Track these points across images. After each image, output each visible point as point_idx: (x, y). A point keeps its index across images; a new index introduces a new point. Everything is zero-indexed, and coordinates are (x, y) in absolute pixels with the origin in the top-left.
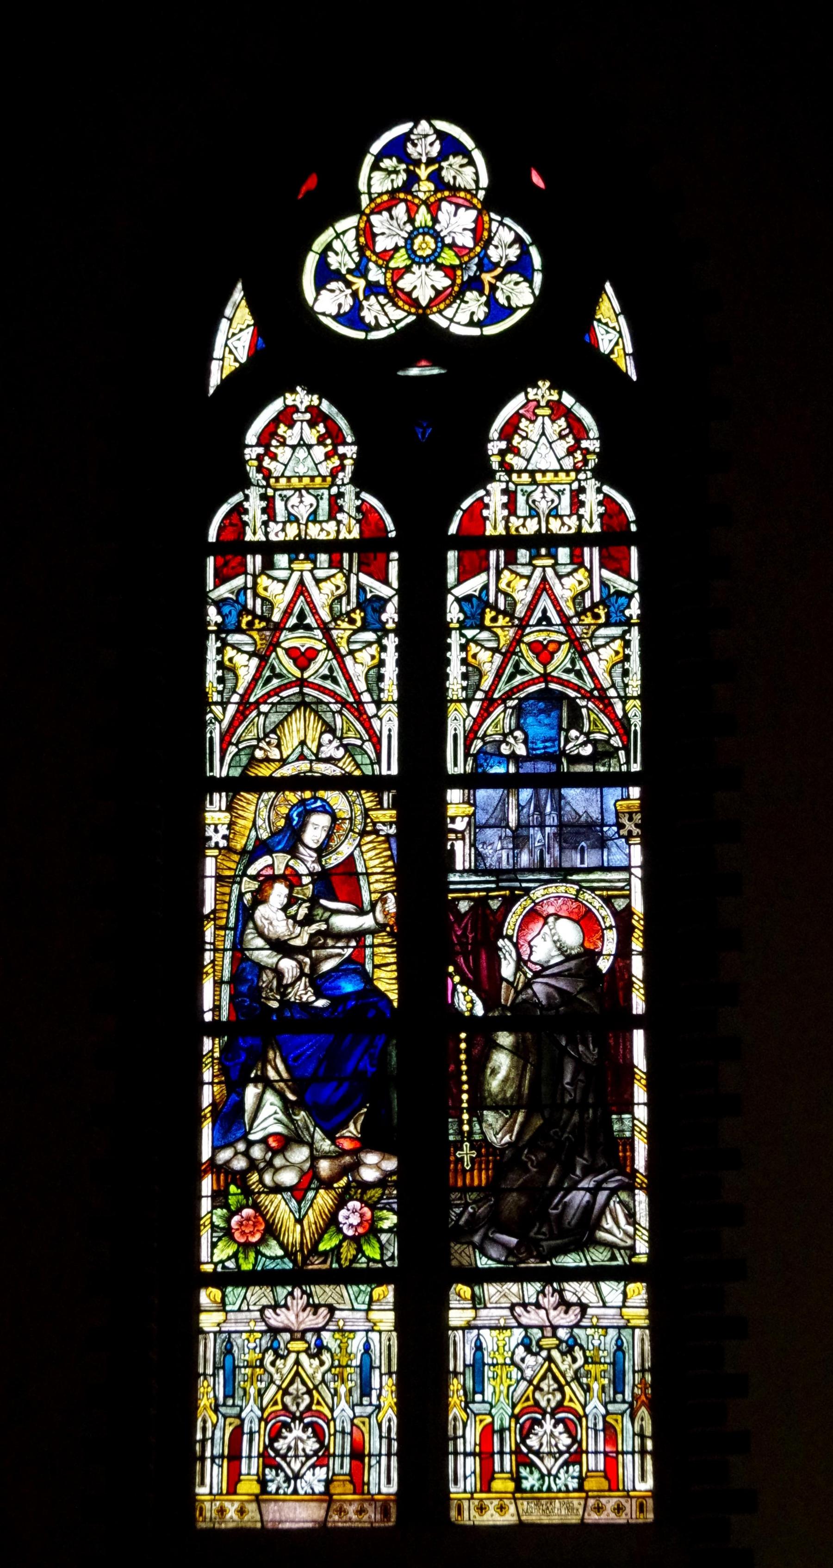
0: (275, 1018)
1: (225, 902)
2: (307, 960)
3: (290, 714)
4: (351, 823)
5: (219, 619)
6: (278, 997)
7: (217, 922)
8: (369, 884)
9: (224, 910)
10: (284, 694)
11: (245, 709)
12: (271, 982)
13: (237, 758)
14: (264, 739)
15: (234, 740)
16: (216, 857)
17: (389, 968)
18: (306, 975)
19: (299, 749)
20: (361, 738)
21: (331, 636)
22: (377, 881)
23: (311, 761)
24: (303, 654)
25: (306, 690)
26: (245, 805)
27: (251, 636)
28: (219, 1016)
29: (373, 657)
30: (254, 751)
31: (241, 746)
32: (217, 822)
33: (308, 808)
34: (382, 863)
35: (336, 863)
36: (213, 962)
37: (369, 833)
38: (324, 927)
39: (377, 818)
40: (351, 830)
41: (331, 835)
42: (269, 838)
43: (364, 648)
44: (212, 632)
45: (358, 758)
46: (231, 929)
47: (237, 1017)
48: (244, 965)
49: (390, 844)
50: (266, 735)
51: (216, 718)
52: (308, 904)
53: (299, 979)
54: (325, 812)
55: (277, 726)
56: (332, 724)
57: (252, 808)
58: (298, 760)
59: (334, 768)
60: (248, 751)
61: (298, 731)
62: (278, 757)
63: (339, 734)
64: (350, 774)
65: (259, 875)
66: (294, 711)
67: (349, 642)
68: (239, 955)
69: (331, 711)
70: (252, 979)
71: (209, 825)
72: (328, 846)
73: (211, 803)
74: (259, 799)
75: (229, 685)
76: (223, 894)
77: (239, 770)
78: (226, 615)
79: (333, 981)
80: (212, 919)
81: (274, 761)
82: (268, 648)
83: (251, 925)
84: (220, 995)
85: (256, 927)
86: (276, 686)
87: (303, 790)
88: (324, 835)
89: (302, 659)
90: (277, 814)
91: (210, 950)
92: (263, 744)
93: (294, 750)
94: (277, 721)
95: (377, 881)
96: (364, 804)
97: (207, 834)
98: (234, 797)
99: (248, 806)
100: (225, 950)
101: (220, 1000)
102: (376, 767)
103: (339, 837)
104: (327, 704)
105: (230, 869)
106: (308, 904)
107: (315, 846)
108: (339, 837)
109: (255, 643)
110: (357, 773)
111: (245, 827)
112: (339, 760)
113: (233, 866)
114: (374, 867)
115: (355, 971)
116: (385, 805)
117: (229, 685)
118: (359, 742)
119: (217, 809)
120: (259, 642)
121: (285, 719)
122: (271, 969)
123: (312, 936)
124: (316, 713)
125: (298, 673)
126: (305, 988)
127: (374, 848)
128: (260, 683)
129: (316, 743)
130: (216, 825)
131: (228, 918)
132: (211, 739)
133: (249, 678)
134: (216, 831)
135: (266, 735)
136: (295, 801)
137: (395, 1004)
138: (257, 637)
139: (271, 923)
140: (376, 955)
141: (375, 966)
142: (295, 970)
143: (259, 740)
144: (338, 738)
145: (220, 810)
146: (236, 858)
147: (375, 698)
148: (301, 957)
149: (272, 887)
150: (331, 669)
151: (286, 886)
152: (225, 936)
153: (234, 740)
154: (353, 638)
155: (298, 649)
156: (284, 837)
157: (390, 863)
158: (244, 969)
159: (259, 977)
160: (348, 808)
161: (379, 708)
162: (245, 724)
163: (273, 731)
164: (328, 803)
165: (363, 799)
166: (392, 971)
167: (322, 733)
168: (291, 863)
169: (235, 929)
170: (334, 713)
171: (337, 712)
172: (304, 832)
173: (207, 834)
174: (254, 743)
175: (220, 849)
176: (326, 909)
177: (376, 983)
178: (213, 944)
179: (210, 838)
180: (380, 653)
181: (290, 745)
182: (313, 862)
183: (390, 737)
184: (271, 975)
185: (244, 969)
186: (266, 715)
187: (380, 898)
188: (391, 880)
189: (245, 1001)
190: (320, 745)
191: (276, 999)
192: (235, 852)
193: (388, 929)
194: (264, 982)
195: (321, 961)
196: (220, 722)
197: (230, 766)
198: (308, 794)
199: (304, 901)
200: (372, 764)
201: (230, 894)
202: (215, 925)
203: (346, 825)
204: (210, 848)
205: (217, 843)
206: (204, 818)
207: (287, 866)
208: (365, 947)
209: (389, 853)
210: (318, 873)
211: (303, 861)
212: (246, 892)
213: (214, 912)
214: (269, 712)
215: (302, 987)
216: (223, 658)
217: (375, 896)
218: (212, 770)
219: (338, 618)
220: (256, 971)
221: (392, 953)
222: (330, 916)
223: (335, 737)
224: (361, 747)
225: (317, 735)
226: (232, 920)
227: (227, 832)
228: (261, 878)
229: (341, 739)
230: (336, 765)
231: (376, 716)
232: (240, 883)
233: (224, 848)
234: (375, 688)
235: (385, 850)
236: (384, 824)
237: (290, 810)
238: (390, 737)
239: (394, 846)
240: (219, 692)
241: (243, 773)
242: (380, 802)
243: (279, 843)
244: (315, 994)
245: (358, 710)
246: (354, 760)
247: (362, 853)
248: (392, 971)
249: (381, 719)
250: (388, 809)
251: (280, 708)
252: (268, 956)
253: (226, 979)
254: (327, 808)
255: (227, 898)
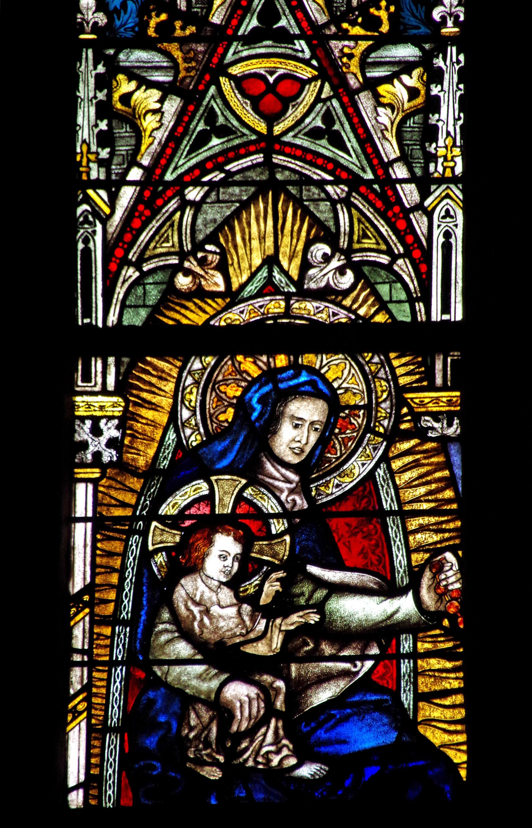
0: (213, 802)
1: (113, 570)
2: (280, 684)
3: (245, 205)
4: (369, 417)
5: (102, 19)
6: (221, 759)
7: (97, 610)
8: (407, 534)
9: (112, 586)
10: (233, 167)
11: (156, 195)
12: (207, 727)
13: (140, 290)
14: (193, 253)
15: (132, 256)
16: (95, 482)
17: (448, 702)
18: (278, 715)
19: (264, 273)
20: (389, 252)
21: (329, 52)
22: (422, 529)
23: (288, 297)
24: (271, 88)
25: (278, 159)
26: (154, 380)
27: (168, 54)
28: (99, 798)
29: (413, 93)
30: (173, 276)
31: (146, 268)
32: (99, 414)
33: (282, 386)
34: (430, 493)
35: (338, 492)
36: (87, 688)
37: (406, 436)
38: (314, 618)
39: (422, 404)
40: (368, 429)
41: (329, 439)
42: (202, 444)
43: (396, 75)
44: (88, 43)
45: (384, 290)
46: (124, 623)
47: (136, 798)
48: (151, 694)
49: (448, 456)
50: (198, 246)
51: (96, 213)
52: (281, 574)
53: (264, 721)
54: (317, 394)
55: (219, 228)
56: (331, 223)
57: (170, 387)
58: (260, 294)
59: (334, 308)
60: (159, 277)
61: (262, 238)
62: (222, 288)
63: (343, 243)
64: (367, 320)
65: (182, 515)
66: (253, 199)
67: (364, 65)
68: (141, 674)
69: (329, 197)
70: (168, 723)
71: (83, 419)
72: (322, 459)
73: (87, 378)
74: (181, 370)
75: (123, 148)
76: (110, 554)
77: (143, 313)
78: (116, 11)
79: (333, 727)
80: (86, 605)
81: (214, 295)
82: (201, 78)
83: (166, 615)
84: (102, 755)
85: (176, 618)
86: (217, 150)
87: (272, 354)
88: (314, 438)
89: (270, 98)
90: (220, 399)
91: (81, 664)
92: (191, 264)
93: (253, 275)
94: (219, 218)
95: (422, 529)
96: (395, 378)
97: (77, 438)
98: (132, 366)
99: (161, 384)
100: (112, 664)
101: (101, 766)
102: (420, 306)
103: (344, 442)
104: (321, 184)
105: (123, 505)
106: (281, 574)
107: (295, 460)
108: (344, 442)
109: (175, 67)
110: (380, 318)
111: (154, 424)
112: (346, 293)
113: (130, 499)
114: (417, 500)
115: (378, 706)
116: (439, 381)
117: (123, 148)
118: (384, 259)
119: (98, 388)
120: (182, 65)
121: (236, 214)
122: (206, 703)
123: (289, 636)
124: (298, 203)
125: (262, 127)
126: (277, 741)
127: (416, 464)
128: (185, 145)
129: (297, 262)
130: (96, 420)
131: (118, 602)
132: (87, 253)
133: (161, 135)
134: (96, 431)
135: (198, 246)
136: (255, 372)
137: (463, 773)
138: (177, 54)
139: (207, 612)
140: (423, 673)
141: (419, 697)
142: (255, 704)
143: (183, 255)
144: (342, 252)
145: (104, 392)
146: (136, 484)
147: (418, 172)
148: (267, 678)
149: (210, 542)
150: (328, 118)
151: (237, 539)
152: (112, 637)
153: (132, 256)
154: (374, 56)
155: (263, 78)
156: (233, 442)
157: (449, 494)
158: (152, 702)
159: (183, 718)
160: (363, 386)
161: (425, 194)
162: (155, 224)
163: (212, 238)
164: (323, 377)
165: (393, 369)
166: (453, 706)
167: (308, 244)
168: (248, 493)
169: (132, 623)
170: (334, 203)
171: (341, 201)
172: (275, 432)
173: (77, 438)
174: (174, 260)
175: (103, 467)
176: (319, 583)
177: (421, 729)
178: (89, 652)
179: (84, 445)
180: (427, 86)
181: (245, 265)
182: (291, 491)
183: (447, 248)
184: (206, 716)
185: (152, 702)
186: (197, 206)
187: (428, 561)
188: (452, 526)
189: (154, 768)
190: (306, 266)
191: (215, 763)
192: (135, 472)
193: (446, 623)
194: (191, 729)
195: (309, 687)
196: (105, 220)
197: (123, 306)
198: (281, 361)
199: (275, 568)
200: (411, 301)
201: (124, 555)
202: (92, 614)
203: (359, 420)
204: (84, 465)
205: (97, 455)
206: (73, 406)
207: (240, 498)
208: (399, 657)
209: (446, 473)
210: (302, 512)
211: (273, 491)
212: (156, 551)
213: (90, 589)
214: (203, 200)
215: (270, 738)
216: (110, 96)
217: (418, 558)
218: (87, 312)
219: (344, 18)
220: (176, 707)
221: (454, 670)
222: (327, 598)
223: (335, 248)
224: (389, 268)
225: (300, 246)
226: (128, 604)
227: (116, 434)
228: (188, 523)
229: (348, 252)
230: (339, 305)
231: (419, 207)
232: (144, 534)
233: (111, 464)
234: (418, 154)
235: (439, 467)
236: (436, 416)
237: (246, 390)
238: (447, 248)
239: (457, 459)
240: (101, 163)
241: (150, 318)
242: (430, 375)
243: (223, 454)
244: (295, 753)
245: (382, 196)
246: (375, 293)
247: (392, 473)
248: (453, 706)
249: (430, 215)
250: (444, 388)
251: (224, 193)
252: (199, 677)
253: (114, 721)
254: (321, 386)
255: (117, 563)
